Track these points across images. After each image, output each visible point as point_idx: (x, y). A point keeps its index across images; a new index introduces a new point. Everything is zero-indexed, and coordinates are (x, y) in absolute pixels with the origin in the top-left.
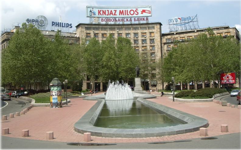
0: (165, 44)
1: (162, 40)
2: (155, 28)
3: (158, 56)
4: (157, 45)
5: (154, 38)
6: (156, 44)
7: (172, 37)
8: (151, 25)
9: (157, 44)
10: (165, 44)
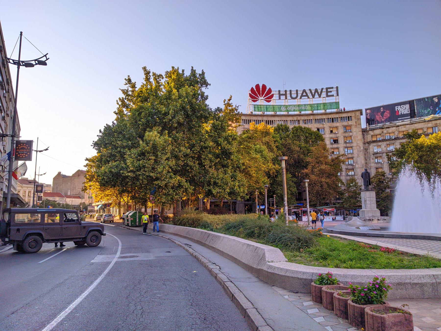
0: (369, 143)
2: (353, 118)
3: (359, 162)
5: (351, 134)
6: (354, 144)
7: (383, 132)
8: (346, 114)
9: (357, 143)
10: (369, 143)
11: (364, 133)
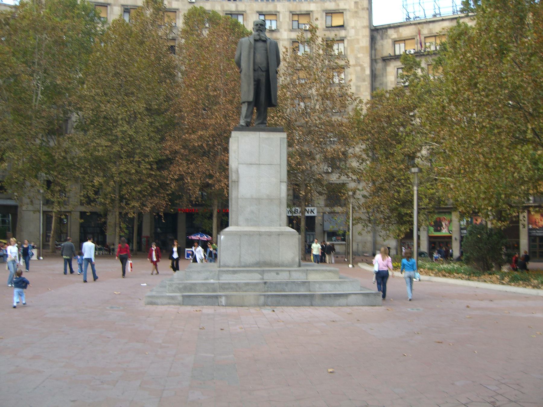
0: (386, 60)
1: (378, 46)
4: (354, 66)
9: (357, 58)
10: (386, 60)
11: (375, 34)
